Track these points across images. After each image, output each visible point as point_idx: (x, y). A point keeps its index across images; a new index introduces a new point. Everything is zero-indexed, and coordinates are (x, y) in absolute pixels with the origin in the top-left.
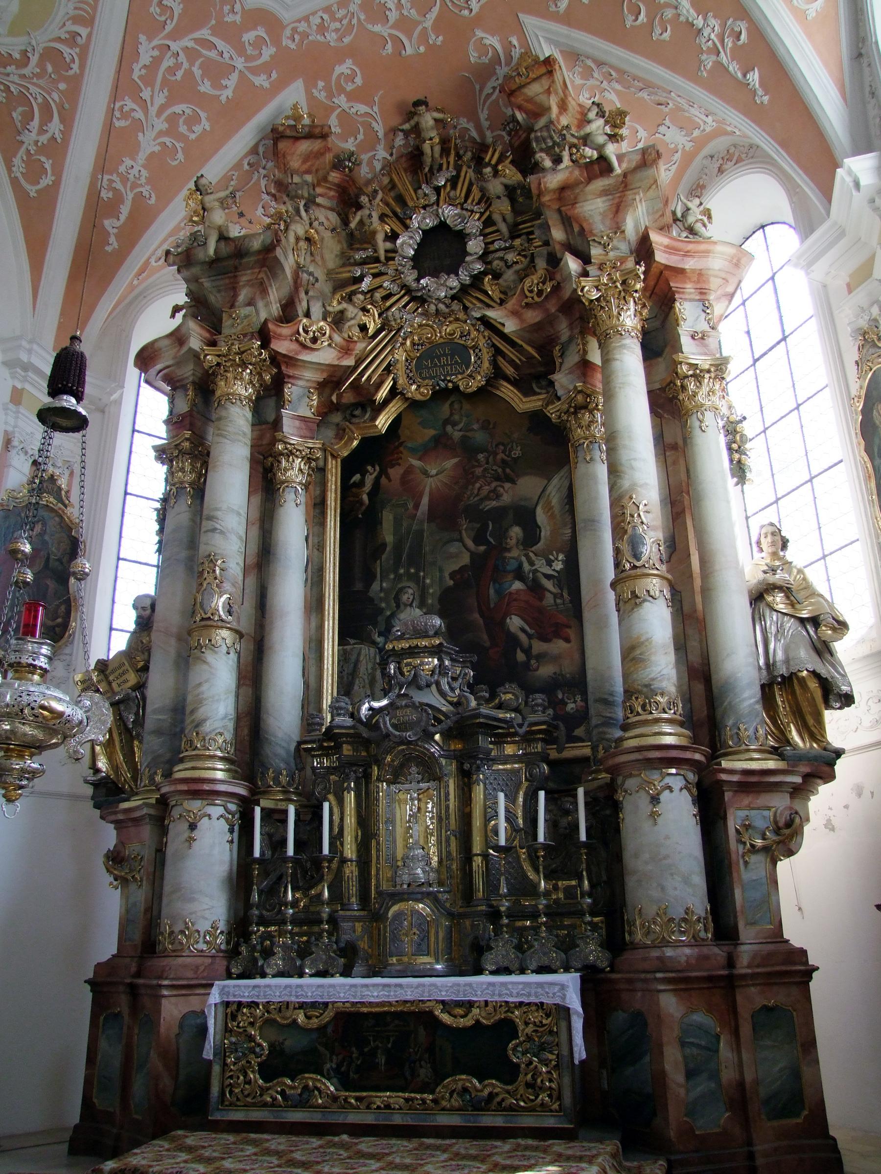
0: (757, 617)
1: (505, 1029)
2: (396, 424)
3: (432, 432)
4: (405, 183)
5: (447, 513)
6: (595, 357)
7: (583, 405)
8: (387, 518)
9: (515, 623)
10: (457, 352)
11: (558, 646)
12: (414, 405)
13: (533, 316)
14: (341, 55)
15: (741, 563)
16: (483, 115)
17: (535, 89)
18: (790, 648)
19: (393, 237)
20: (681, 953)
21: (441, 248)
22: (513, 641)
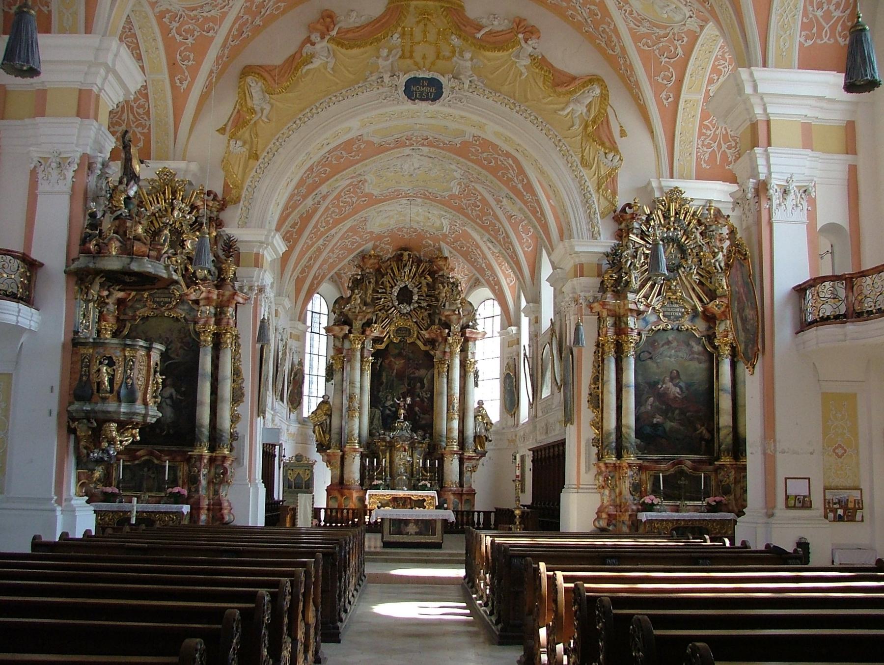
0: (475, 421)
1: (424, 500)
2: (387, 346)
3: (397, 351)
4: (394, 265)
5: (400, 376)
6: (447, 350)
7: (442, 362)
8: (384, 374)
9: (417, 409)
10: (408, 331)
11: (427, 416)
12: (392, 342)
13: (433, 336)
14: (386, 237)
15: (473, 404)
16: (422, 254)
17: (440, 263)
18: (481, 430)
19: (392, 287)
20: (454, 488)
21: (405, 296)
22: (416, 414)
